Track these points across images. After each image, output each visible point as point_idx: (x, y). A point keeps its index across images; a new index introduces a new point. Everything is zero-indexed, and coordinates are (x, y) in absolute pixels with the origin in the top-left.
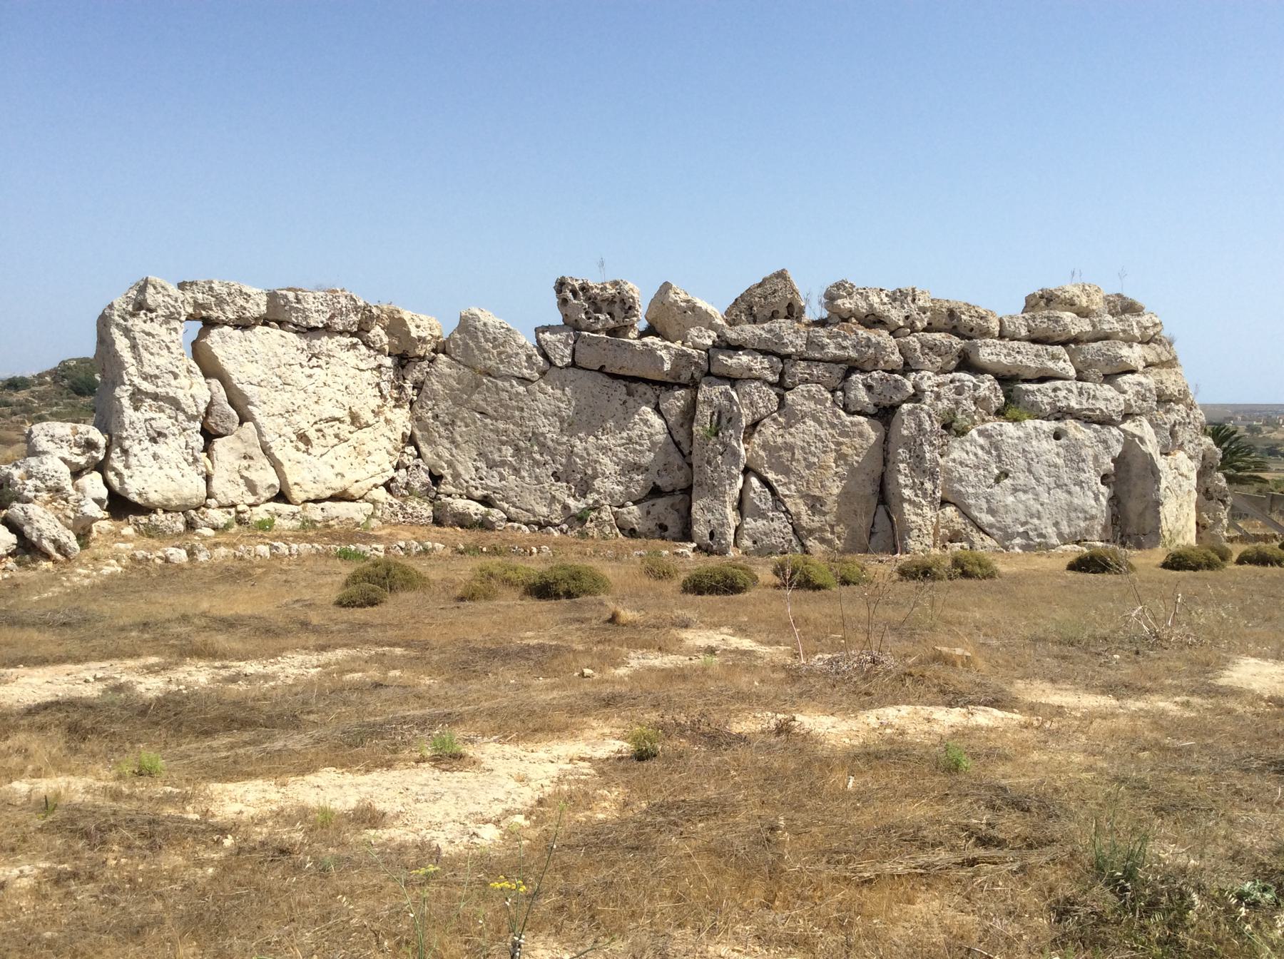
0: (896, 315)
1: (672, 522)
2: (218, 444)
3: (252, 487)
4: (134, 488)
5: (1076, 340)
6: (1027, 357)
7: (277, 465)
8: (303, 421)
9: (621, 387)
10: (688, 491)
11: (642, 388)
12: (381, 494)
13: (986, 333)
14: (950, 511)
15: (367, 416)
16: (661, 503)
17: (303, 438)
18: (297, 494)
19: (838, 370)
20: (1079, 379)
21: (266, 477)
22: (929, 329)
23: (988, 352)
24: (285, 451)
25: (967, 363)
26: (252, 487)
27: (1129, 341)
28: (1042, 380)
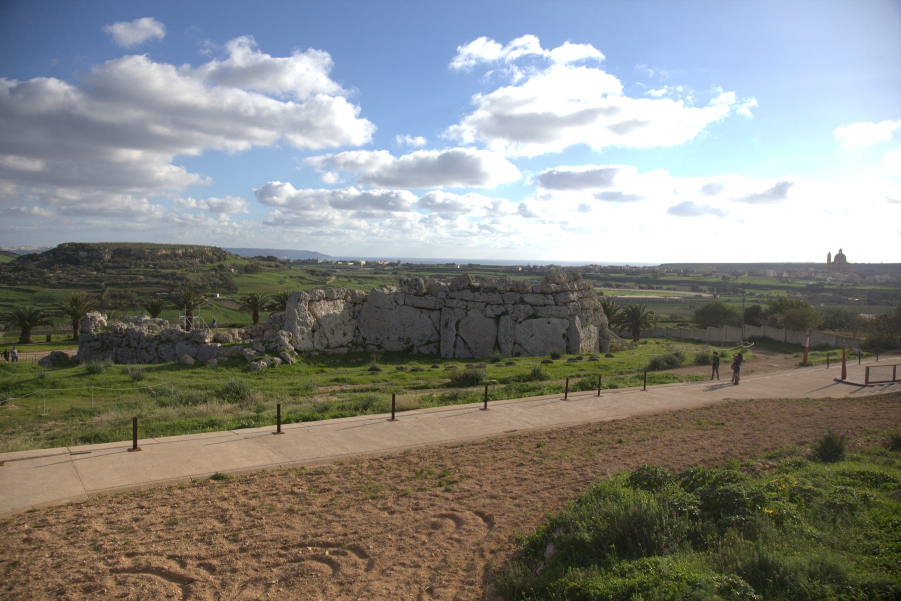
0: (501, 288)
1: (435, 351)
2: (315, 333)
3: (322, 344)
4: (298, 347)
5: (557, 293)
6: (540, 299)
7: (327, 338)
8: (332, 325)
9: (418, 312)
10: (439, 342)
11: (424, 311)
12: (350, 345)
13: (527, 292)
14: (516, 346)
15: (346, 322)
16: (431, 346)
17: (333, 330)
18: (332, 346)
19: (483, 305)
20: (556, 304)
21: (325, 342)
22: (510, 291)
23: (529, 298)
24: (329, 335)
25: (522, 301)
26: (322, 344)
27: (572, 292)
28: (545, 305)
